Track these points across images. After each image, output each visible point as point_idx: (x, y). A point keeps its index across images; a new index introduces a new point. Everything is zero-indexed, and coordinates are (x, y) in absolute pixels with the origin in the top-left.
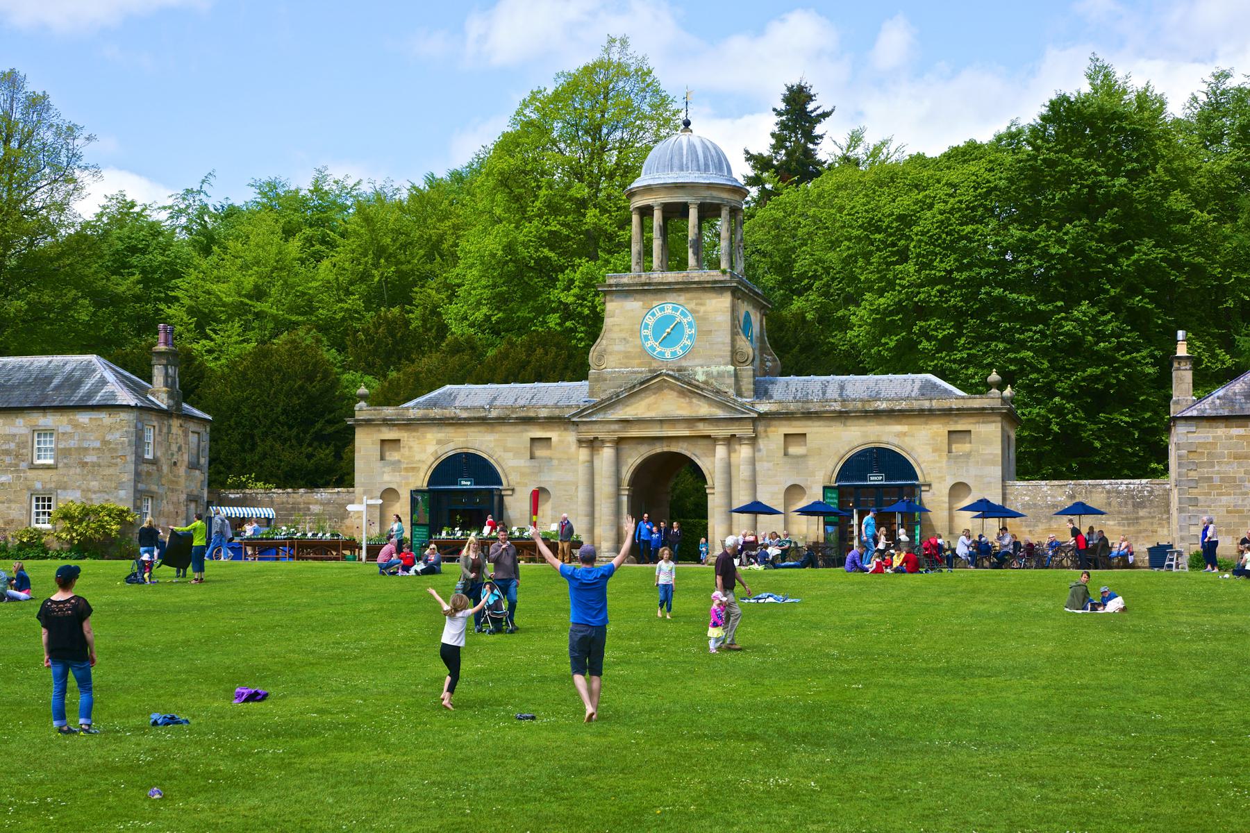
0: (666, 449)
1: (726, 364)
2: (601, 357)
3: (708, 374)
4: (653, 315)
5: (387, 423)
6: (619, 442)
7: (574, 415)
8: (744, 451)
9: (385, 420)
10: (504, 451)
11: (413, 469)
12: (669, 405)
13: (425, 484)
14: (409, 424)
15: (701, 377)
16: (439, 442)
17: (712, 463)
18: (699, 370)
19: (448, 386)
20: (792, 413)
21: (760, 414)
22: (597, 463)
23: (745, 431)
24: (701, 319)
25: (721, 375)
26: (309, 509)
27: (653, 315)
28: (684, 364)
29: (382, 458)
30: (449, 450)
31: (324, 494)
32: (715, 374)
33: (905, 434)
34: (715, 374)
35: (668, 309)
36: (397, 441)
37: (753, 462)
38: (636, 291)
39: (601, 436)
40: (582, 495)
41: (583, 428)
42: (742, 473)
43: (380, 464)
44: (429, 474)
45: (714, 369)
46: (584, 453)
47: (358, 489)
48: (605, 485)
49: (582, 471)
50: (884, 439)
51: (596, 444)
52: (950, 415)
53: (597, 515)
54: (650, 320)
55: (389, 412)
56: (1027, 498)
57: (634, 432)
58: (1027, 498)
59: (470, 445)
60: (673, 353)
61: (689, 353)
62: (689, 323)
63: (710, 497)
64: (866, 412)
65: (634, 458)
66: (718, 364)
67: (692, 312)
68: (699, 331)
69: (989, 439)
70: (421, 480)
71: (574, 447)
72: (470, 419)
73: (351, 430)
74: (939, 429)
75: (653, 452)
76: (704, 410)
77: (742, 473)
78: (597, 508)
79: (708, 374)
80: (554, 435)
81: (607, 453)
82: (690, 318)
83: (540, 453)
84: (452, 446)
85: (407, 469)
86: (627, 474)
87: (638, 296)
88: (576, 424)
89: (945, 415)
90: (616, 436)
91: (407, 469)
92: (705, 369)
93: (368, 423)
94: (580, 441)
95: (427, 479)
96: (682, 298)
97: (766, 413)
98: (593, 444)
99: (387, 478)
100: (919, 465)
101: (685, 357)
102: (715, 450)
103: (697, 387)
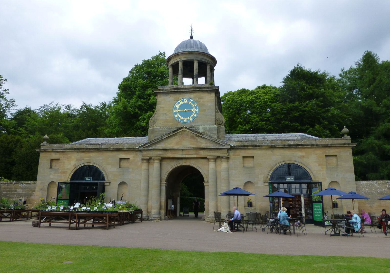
0: (184, 164)
1: (213, 125)
2: (154, 122)
3: (204, 129)
4: (179, 103)
5: (54, 151)
6: (162, 160)
7: (140, 147)
8: (224, 165)
9: (53, 149)
10: (107, 164)
11: (64, 172)
12: (187, 142)
13: (69, 180)
14: (64, 151)
15: (201, 131)
16: (77, 160)
17: (207, 169)
18: (201, 127)
19: (88, 138)
20: (247, 146)
21: (231, 147)
22: (150, 170)
23: (223, 154)
24: (200, 105)
25: (210, 129)
26: (16, 191)
27: (179, 103)
28: (193, 125)
29: (51, 167)
30: (81, 164)
31: (23, 184)
32: (208, 129)
33: (303, 157)
34: (208, 129)
35: (186, 101)
36: (58, 159)
37: (228, 170)
38: (171, 93)
39: (153, 157)
40: (143, 186)
41: (144, 153)
42: (224, 175)
43: (50, 170)
44: (71, 175)
45: (208, 127)
46: (144, 166)
47: (38, 182)
48: (154, 181)
49: (143, 174)
50: (293, 159)
51: (151, 161)
52: (327, 147)
53: (150, 195)
54: (177, 106)
55: (56, 146)
56: (367, 189)
57: (169, 155)
58: (367, 189)
59: (91, 161)
60: (188, 120)
61: (195, 119)
62: (195, 107)
63: (206, 188)
64: (284, 145)
65: (169, 167)
66: (210, 125)
67: (197, 102)
68: (199, 110)
69: (346, 159)
70: (67, 178)
71: (140, 163)
72: (92, 149)
73: (38, 155)
74: (320, 152)
75: (178, 165)
76: (203, 144)
77: (224, 175)
78: (150, 192)
79: (204, 129)
80: (131, 156)
81: (156, 165)
82: (196, 105)
83: (124, 164)
84: (83, 161)
85: (61, 173)
86: (165, 177)
87: (172, 95)
88: (140, 151)
89: (324, 147)
90: (160, 157)
91: (61, 173)
92: (203, 127)
93: (45, 150)
94: (142, 159)
95: (70, 177)
96: (192, 95)
97: (234, 146)
98: (149, 160)
99: (52, 176)
100: (312, 172)
101: (193, 121)
102: (208, 164)
103: (200, 134)
